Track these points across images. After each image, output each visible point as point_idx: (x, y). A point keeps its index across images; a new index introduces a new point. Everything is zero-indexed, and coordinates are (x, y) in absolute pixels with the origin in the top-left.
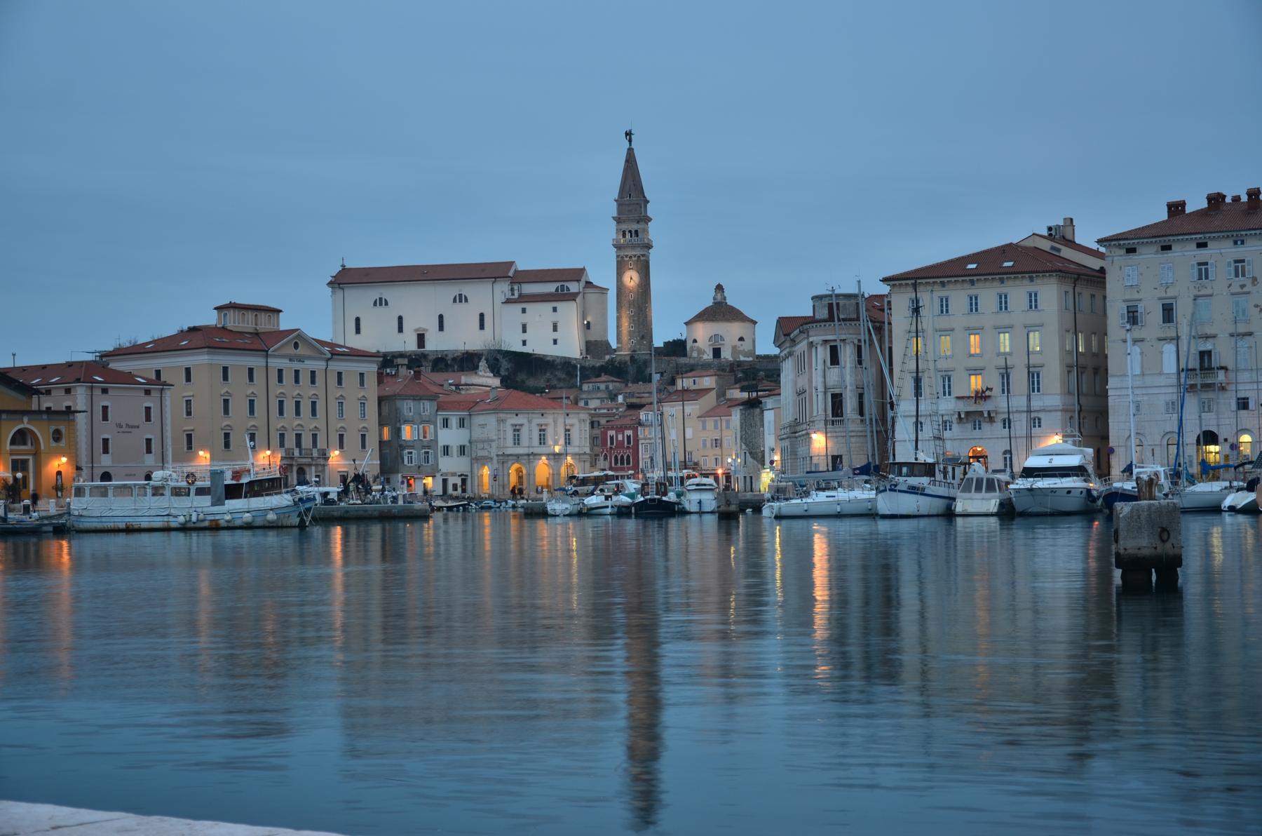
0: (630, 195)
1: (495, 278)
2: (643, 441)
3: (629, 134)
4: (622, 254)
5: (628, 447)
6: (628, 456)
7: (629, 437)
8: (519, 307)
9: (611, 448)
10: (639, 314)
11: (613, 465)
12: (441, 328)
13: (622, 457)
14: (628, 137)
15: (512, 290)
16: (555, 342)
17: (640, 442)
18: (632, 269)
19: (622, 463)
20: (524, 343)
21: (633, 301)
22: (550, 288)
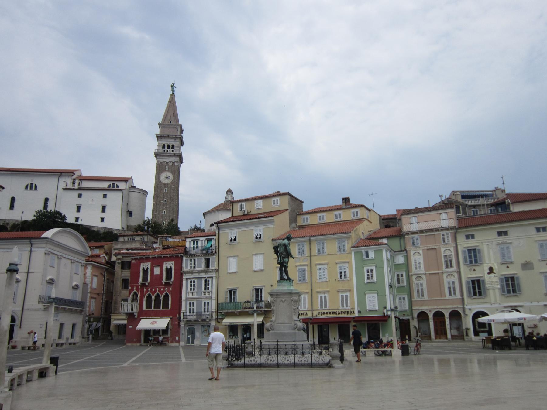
0: (170, 122)
1: (61, 173)
4: (161, 160)
5: (167, 284)
6: (166, 296)
7: (169, 271)
8: (76, 193)
9: (143, 285)
10: (170, 203)
11: (144, 308)
12: (12, 207)
13: (158, 297)
15: (74, 183)
16: (102, 220)
17: (185, 276)
18: (168, 171)
19: (157, 305)
20: (77, 219)
21: (167, 193)
22: (105, 185)
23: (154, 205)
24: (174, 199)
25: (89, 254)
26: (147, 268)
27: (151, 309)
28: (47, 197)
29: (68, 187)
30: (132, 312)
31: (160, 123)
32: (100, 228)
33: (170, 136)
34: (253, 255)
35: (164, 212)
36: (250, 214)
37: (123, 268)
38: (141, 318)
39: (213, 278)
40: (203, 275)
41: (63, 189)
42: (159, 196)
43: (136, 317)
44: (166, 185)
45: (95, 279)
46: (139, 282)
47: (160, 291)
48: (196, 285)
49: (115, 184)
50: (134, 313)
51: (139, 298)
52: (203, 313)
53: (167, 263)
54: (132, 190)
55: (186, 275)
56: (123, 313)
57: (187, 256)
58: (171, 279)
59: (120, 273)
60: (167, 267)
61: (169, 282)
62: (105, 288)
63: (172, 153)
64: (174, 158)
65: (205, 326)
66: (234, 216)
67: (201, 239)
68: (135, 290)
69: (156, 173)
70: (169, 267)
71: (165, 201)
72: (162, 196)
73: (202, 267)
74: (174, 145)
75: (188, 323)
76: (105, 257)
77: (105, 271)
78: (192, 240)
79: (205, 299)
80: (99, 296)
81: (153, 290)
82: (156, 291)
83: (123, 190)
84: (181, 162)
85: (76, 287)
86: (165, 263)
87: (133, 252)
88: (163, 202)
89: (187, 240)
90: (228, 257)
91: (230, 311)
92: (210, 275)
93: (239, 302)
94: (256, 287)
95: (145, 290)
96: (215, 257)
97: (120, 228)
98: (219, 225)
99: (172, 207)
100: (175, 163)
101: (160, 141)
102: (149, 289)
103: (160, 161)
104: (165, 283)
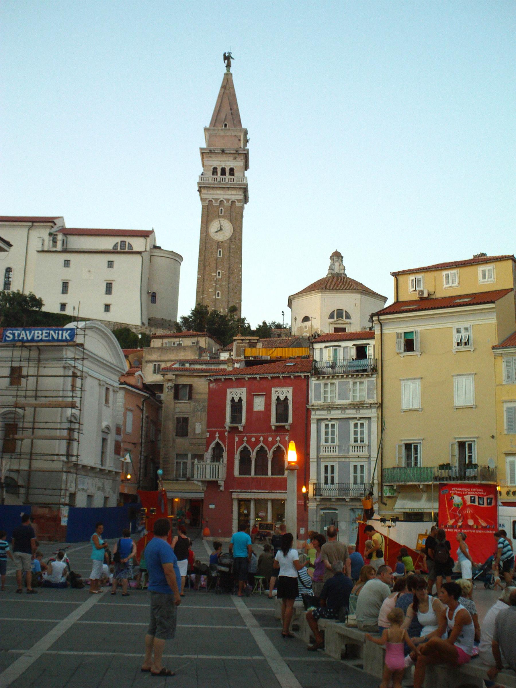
0: (226, 126)
2: (322, 414)
3: (227, 58)
4: (210, 197)
7: (282, 404)
9: (234, 430)
11: (236, 473)
13: (262, 452)
14: (226, 61)
15: (55, 242)
16: (107, 308)
17: (315, 416)
18: (223, 217)
19: (261, 468)
20: (63, 306)
21: (222, 259)
22: (108, 243)
23: (198, 279)
24: (235, 270)
25: (124, 370)
26: (240, 398)
27: (250, 475)
28: (9, 266)
29: (46, 249)
30: (214, 479)
31: (208, 127)
32: (106, 322)
33: (226, 152)
34: (453, 376)
35: (218, 293)
36: (433, 297)
37: (176, 397)
38: (231, 491)
39: (372, 419)
40: (351, 413)
41: (38, 251)
42: (208, 263)
43: (222, 488)
44: (219, 244)
45: (130, 416)
46: (225, 425)
47: (265, 441)
48: (336, 433)
49: (125, 242)
50: (219, 482)
51: (225, 454)
52: (352, 486)
53: (279, 389)
54: (156, 252)
55: (318, 413)
56: (198, 481)
57: (319, 378)
58: (286, 420)
59: (172, 407)
60: (278, 397)
61: (284, 427)
62: (144, 432)
63: (231, 185)
64: (234, 192)
65: (356, 510)
66: (400, 302)
67: (344, 344)
68: (217, 440)
69: (202, 222)
70: (282, 398)
71: (219, 272)
72: (213, 264)
73: (349, 399)
74: (234, 168)
75: (323, 503)
76: (141, 376)
77: (144, 401)
78: (326, 347)
79: (357, 460)
80: (135, 447)
81: (253, 439)
82: (257, 442)
83: (143, 253)
84: (246, 199)
85: (106, 431)
86: (274, 390)
87: (192, 367)
88: (216, 276)
89: (317, 346)
90: (400, 380)
91: (410, 483)
92: (364, 413)
93: (427, 468)
94: (460, 438)
95: (237, 439)
96: (374, 379)
97: (139, 323)
98: (382, 317)
99: (231, 285)
100: (237, 203)
101: (208, 161)
102: (245, 439)
103: (208, 200)
104: (277, 427)
